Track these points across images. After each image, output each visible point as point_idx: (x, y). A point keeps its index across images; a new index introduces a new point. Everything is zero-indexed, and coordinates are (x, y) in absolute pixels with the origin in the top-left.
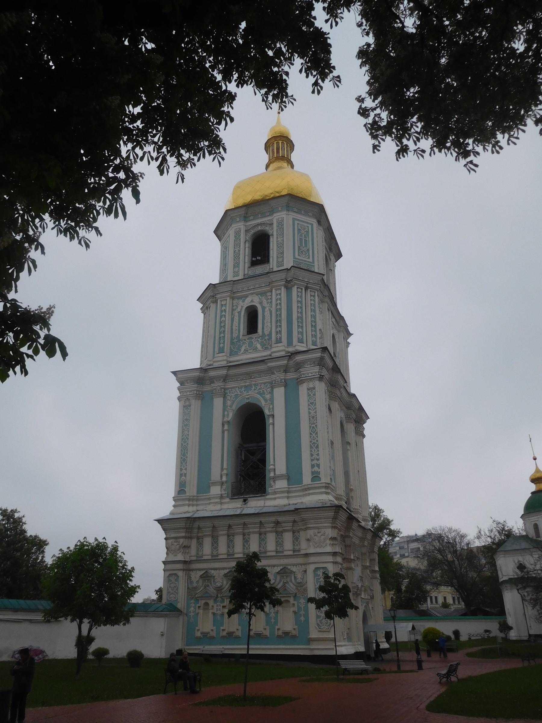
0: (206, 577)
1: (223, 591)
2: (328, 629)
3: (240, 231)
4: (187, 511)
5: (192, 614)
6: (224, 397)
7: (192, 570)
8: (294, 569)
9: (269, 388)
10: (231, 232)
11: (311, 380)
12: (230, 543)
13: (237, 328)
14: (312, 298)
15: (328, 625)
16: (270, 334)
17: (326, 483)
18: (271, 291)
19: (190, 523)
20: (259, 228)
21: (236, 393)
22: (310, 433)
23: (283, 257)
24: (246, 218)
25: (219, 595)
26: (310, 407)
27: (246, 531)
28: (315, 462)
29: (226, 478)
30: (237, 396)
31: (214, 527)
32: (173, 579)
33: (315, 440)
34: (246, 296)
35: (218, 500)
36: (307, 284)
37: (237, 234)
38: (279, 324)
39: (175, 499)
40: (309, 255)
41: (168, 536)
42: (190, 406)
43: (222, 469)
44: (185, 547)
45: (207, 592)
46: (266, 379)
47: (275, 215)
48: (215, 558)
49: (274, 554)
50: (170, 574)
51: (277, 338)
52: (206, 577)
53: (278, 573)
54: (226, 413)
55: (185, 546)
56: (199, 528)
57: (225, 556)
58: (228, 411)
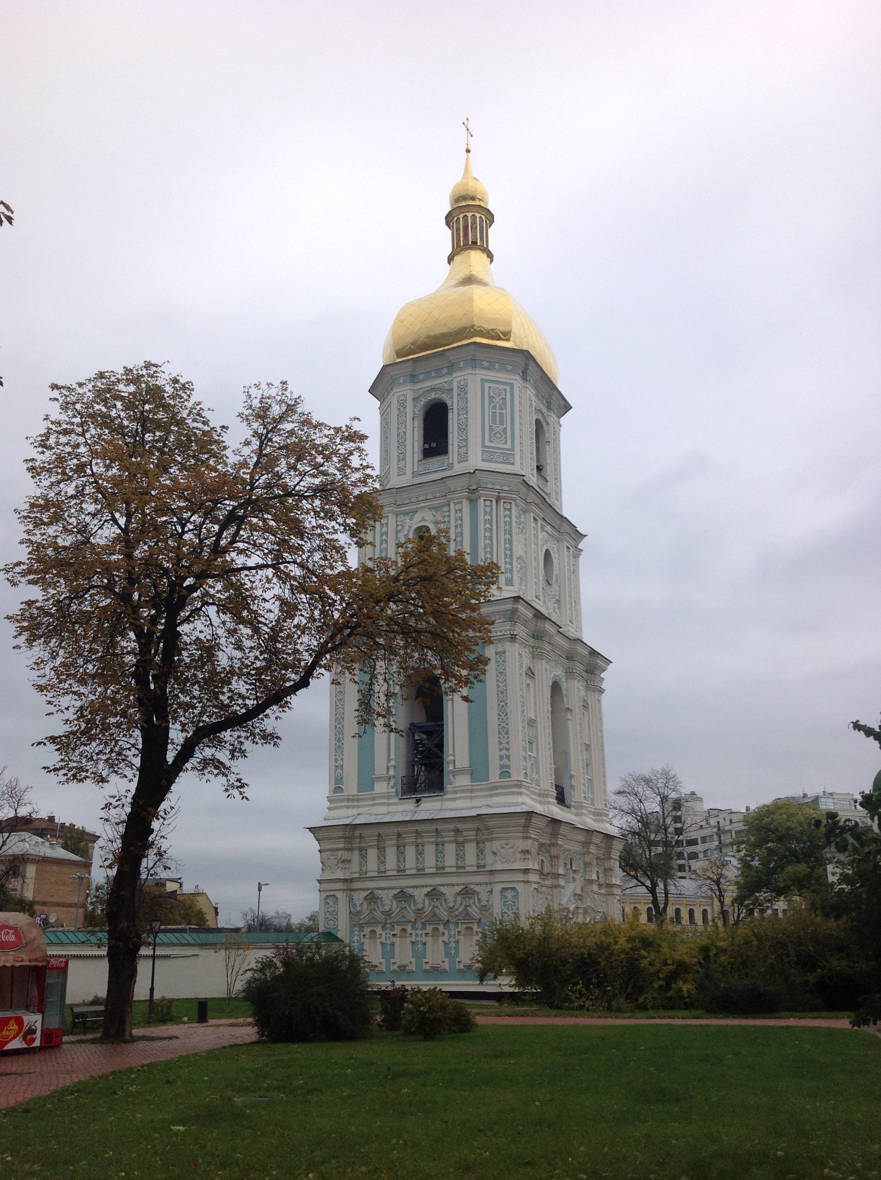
0: (372, 898)
1: (393, 915)
3: (405, 401)
4: (345, 816)
5: (356, 944)
8: (478, 889)
10: (393, 399)
11: (500, 640)
14: (507, 513)
18: (449, 505)
19: (350, 832)
20: (433, 395)
23: (466, 446)
24: (413, 378)
25: (388, 921)
26: (498, 678)
28: (504, 752)
29: (394, 771)
31: (379, 835)
32: (330, 901)
34: (415, 512)
36: (499, 493)
37: (402, 404)
40: (506, 438)
41: (323, 848)
43: (389, 760)
44: (344, 861)
45: (373, 918)
48: (382, 875)
49: (454, 870)
50: (327, 896)
52: (372, 898)
53: (458, 894)
56: (361, 837)
57: (395, 873)
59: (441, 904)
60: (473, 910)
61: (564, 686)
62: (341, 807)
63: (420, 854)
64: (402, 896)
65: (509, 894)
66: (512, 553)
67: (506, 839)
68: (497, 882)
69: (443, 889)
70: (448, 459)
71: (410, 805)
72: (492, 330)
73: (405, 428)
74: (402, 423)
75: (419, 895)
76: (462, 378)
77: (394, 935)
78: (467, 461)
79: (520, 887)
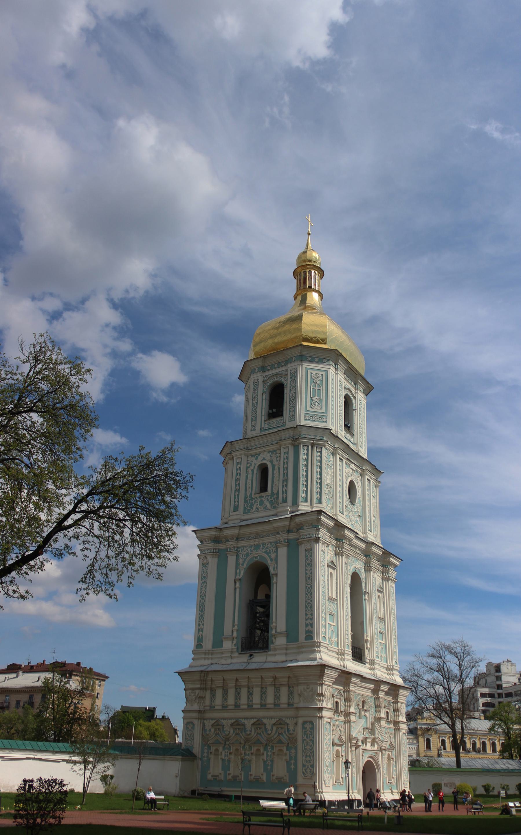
0: (218, 725)
2: (311, 777)
3: (258, 383)
4: (204, 664)
5: (205, 759)
6: (237, 556)
7: (206, 719)
8: (288, 721)
9: (274, 547)
13: (250, 486)
15: (311, 773)
16: (278, 494)
18: (280, 449)
20: (276, 379)
21: (247, 552)
22: (306, 593)
23: (295, 411)
24: (263, 369)
28: (309, 621)
30: (247, 555)
33: (310, 601)
35: (229, 655)
36: (313, 441)
37: (256, 385)
38: (285, 483)
39: (194, 652)
42: (208, 564)
43: (234, 626)
46: (272, 539)
47: (289, 365)
48: (225, 707)
51: (283, 498)
53: (274, 724)
54: (238, 571)
55: (200, 697)
56: (212, 681)
58: (240, 569)
59: (263, 732)
60: (284, 737)
61: (362, 575)
62: (201, 659)
65: (308, 726)
66: (321, 481)
69: (265, 721)
70: (283, 419)
71: (244, 658)
72: (315, 337)
73: (257, 400)
74: (255, 397)
75: (248, 724)
76: (293, 368)
78: (294, 420)
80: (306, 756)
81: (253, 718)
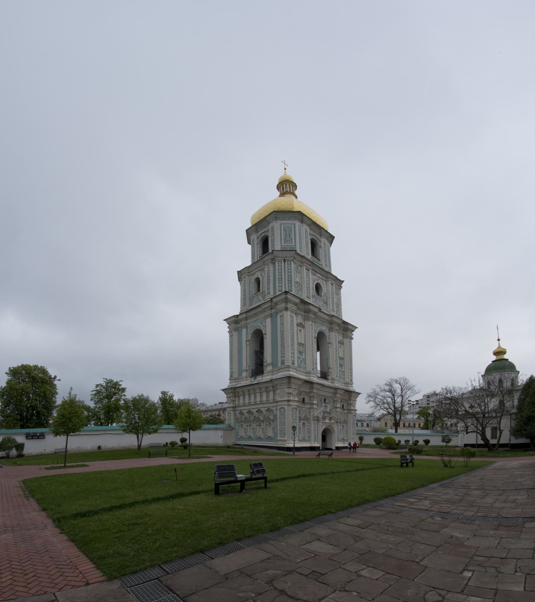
0: (241, 413)
8: (273, 408)
11: (281, 311)
12: (250, 399)
17: (287, 365)
23: (274, 247)
27: (255, 392)
31: (243, 391)
35: (245, 379)
39: (230, 380)
44: (233, 401)
45: (242, 420)
46: (263, 315)
53: (266, 411)
56: (238, 392)
63: (255, 397)
64: (249, 412)
65: (282, 410)
67: (282, 389)
68: (278, 406)
71: (252, 379)
77: (247, 426)
79: (286, 407)
80: (281, 425)
81: (257, 408)
